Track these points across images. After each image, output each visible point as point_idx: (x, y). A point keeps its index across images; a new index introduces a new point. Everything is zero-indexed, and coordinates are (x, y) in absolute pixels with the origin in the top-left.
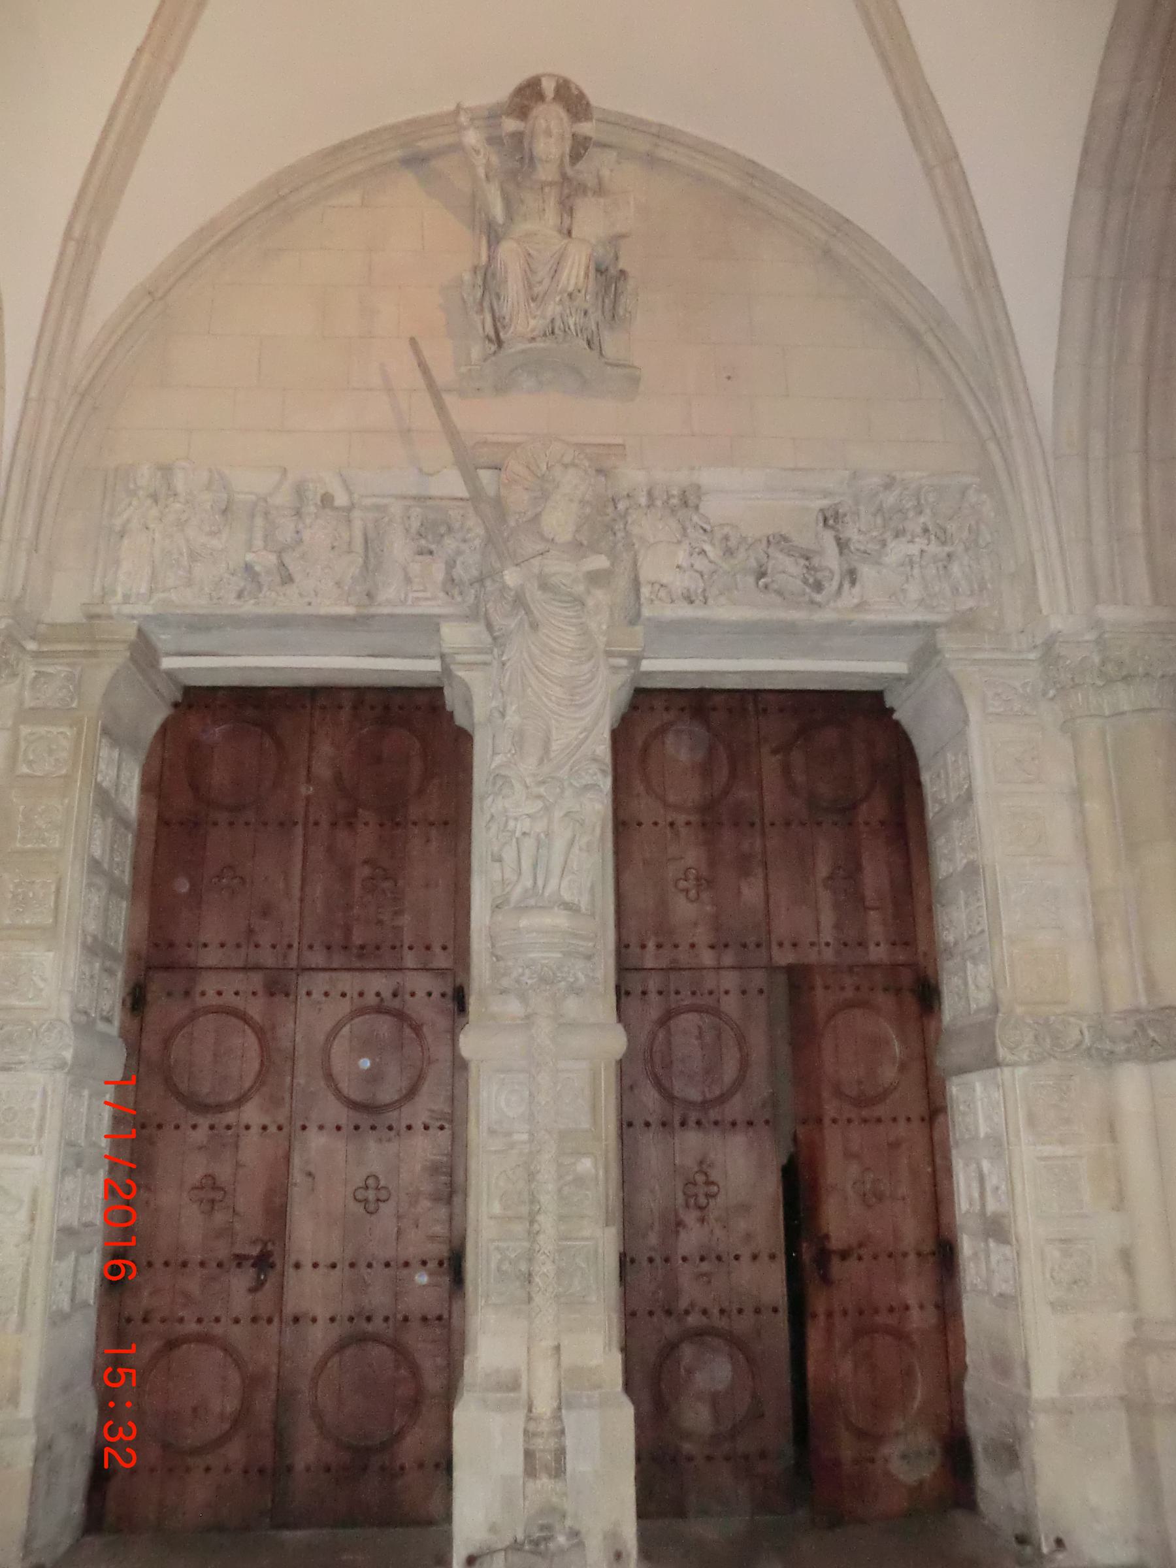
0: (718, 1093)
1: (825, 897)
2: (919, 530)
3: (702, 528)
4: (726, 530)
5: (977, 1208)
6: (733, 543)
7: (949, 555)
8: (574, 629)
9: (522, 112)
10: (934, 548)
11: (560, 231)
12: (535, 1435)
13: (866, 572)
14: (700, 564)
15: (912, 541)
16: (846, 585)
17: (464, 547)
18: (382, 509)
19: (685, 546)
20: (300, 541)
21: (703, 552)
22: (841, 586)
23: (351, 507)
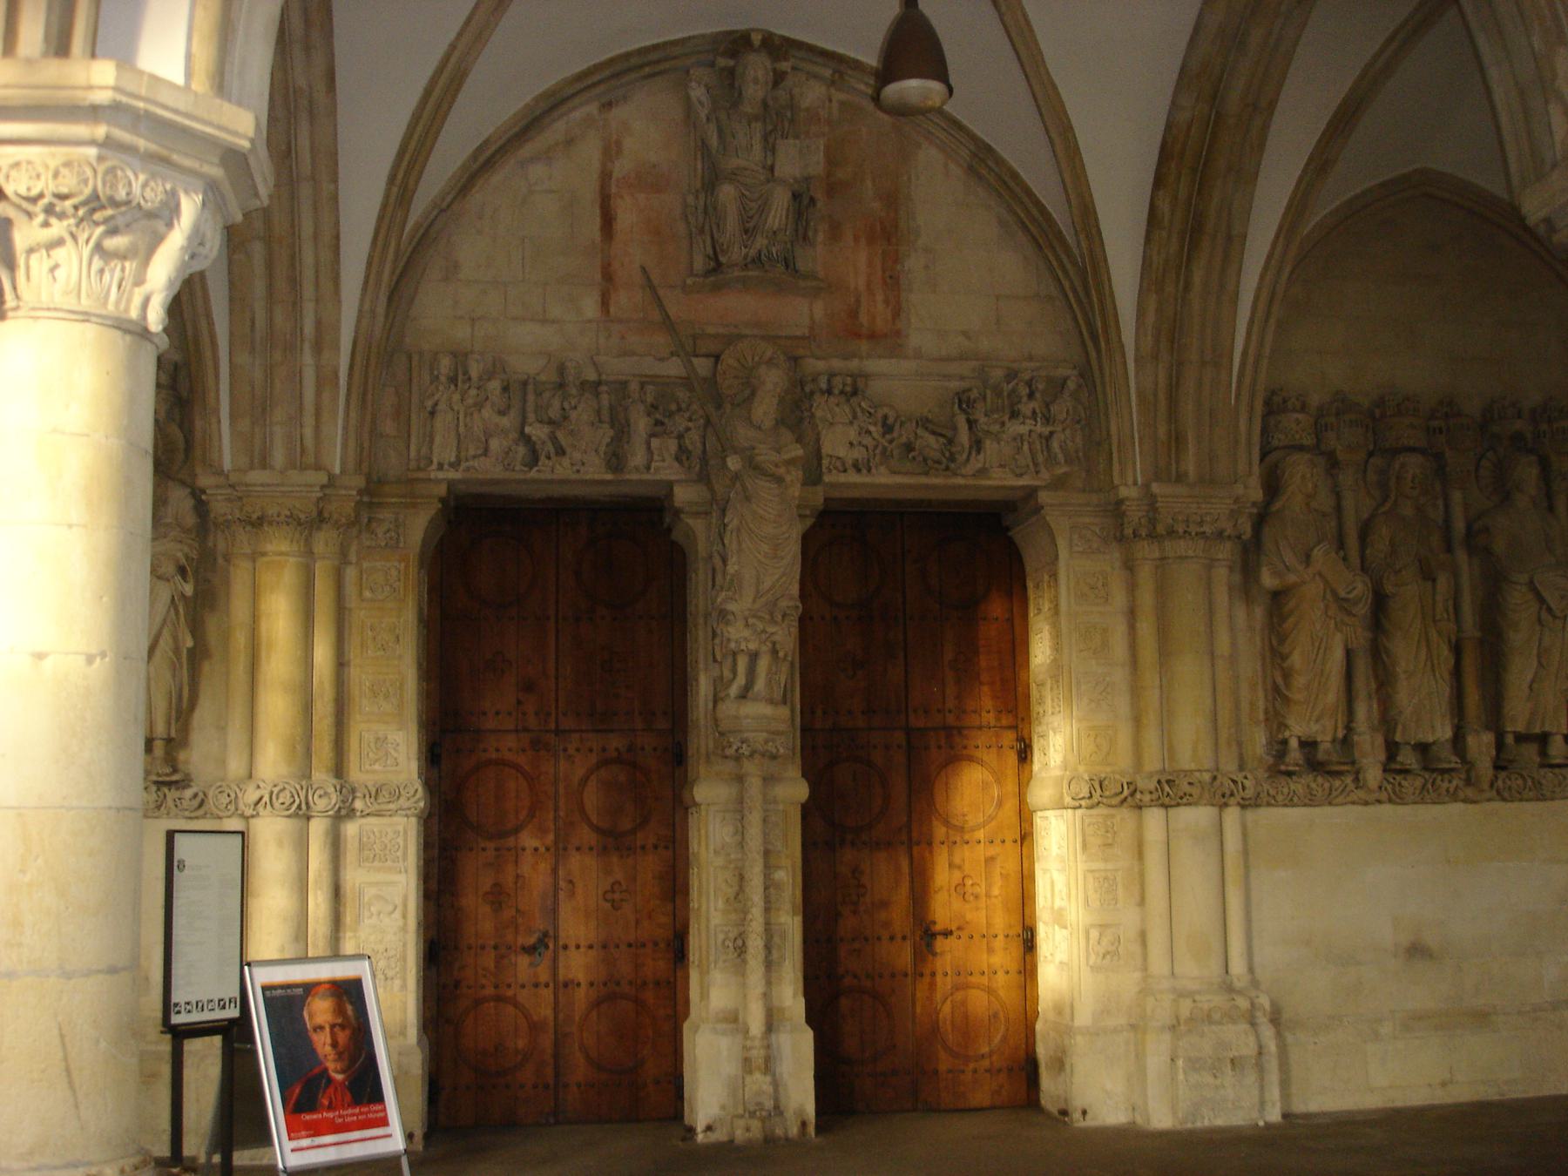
2: (1029, 413)
4: (886, 410)
5: (1049, 903)
6: (890, 421)
7: (1051, 433)
9: (733, 54)
10: (1041, 428)
11: (764, 167)
12: (751, 1048)
13: (988, 444)
14: (867, 441)
15: (1023, 423)
16: (974, 453)
17: (690, 424)
18: (625, 384)
19: (856, 427)
20: (565, 418)
21: (869, 432)
22: (970, 453)
23: (599, 383)
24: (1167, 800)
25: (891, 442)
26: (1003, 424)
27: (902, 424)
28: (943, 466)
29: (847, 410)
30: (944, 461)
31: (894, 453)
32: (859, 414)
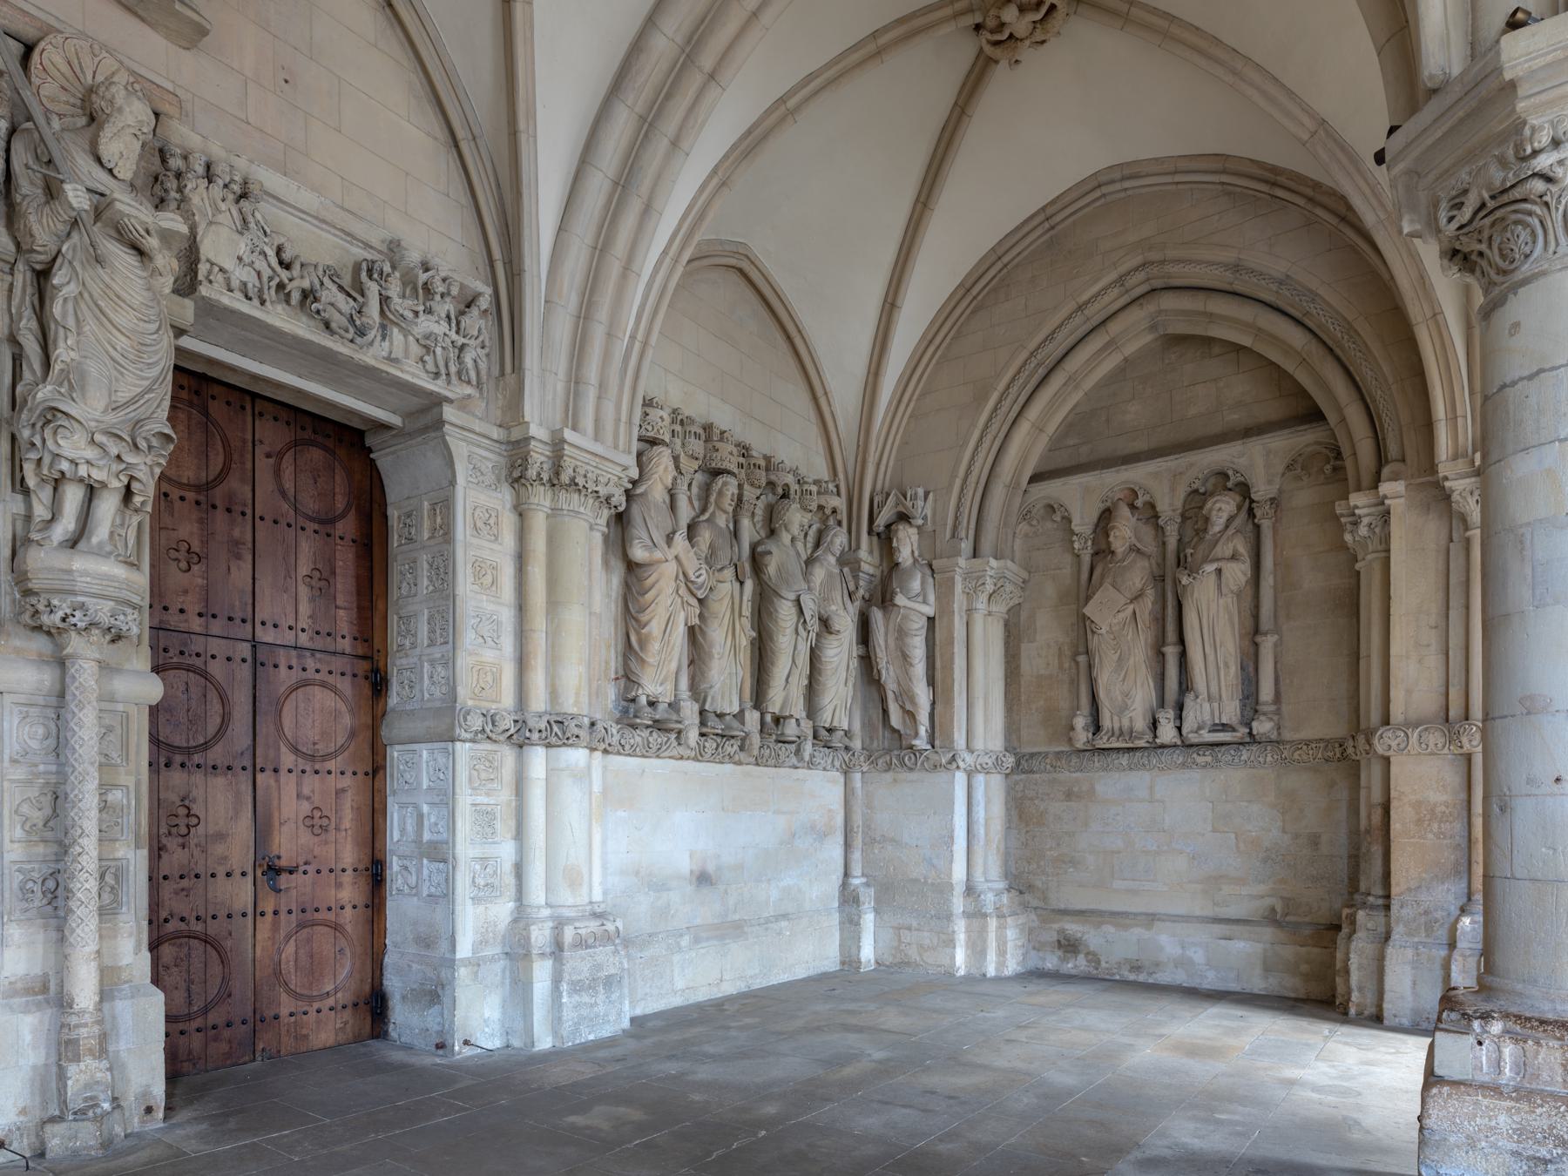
0: (202, 741)
1: (304, 592)
8: (139, 281)
24: (554, 740)
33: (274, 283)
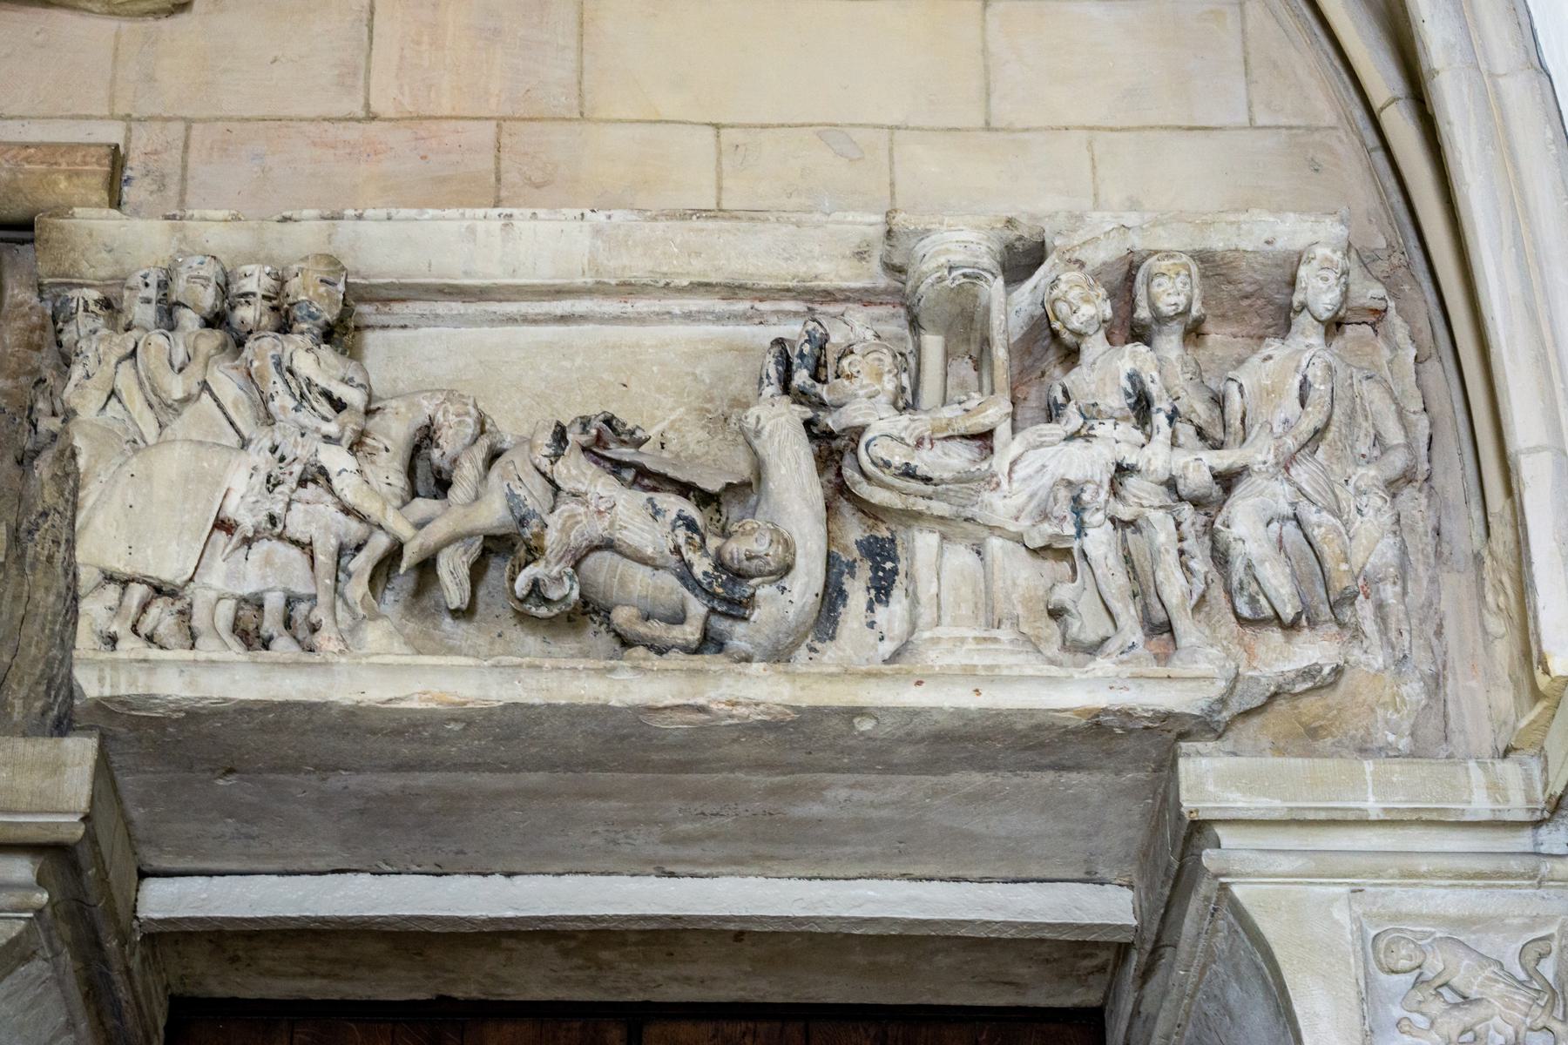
2: (1116, 401)
3: (327, 395)
21: (316, 476)
25: (420, 526)
26: (984, 438)
27: (494, 456)
28: (690, 632)
29: (227, 384)
30: (697, 608)
31: (443, 569)
32: (282, 402)
33: (362, 564)
